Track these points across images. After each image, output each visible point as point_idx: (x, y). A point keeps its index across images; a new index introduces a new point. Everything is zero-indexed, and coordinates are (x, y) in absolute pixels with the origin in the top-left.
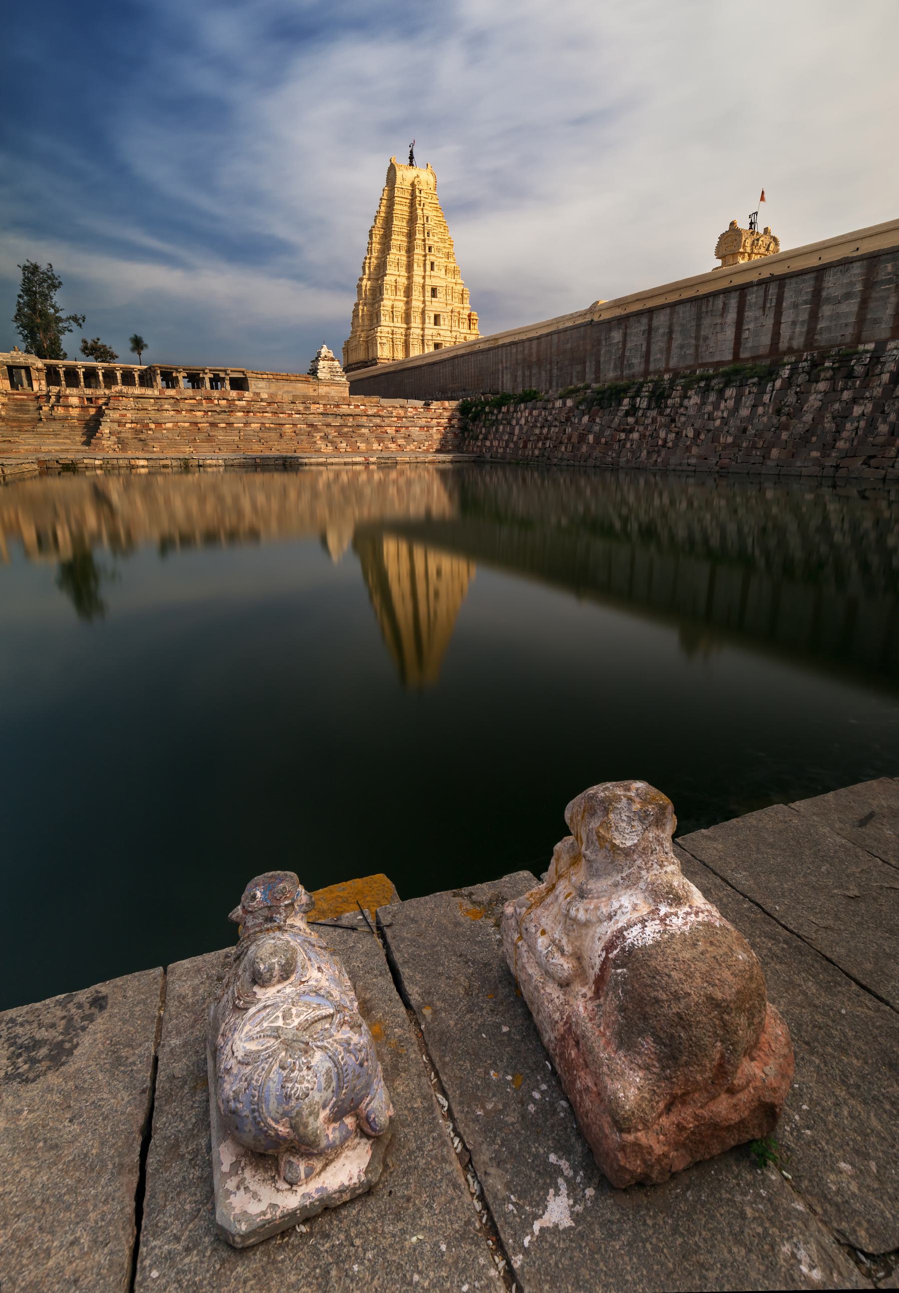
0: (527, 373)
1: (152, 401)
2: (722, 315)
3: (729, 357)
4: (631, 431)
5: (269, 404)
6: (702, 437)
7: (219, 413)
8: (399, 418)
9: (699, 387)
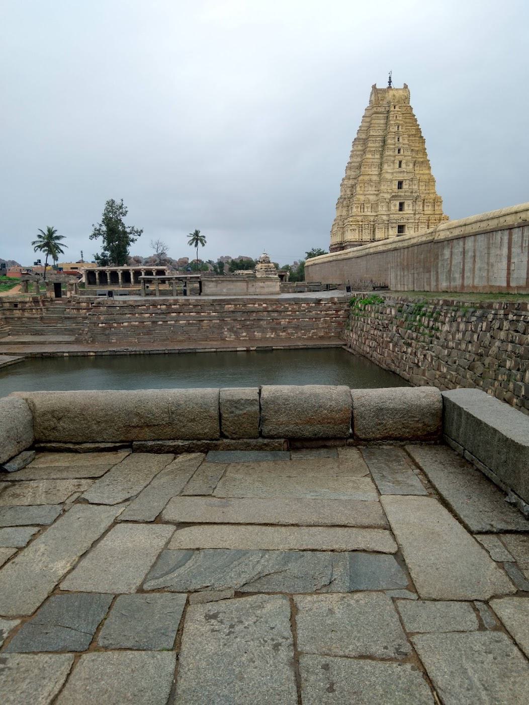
0: (402, 274)
1: (118, 308)
2: (500, 249)
3: (505, 284)
4: (409, 345)
5: (195, 306)
6: (434, 363)
7: (160, 314)
8: (294, 311)
9: (452, 316)
